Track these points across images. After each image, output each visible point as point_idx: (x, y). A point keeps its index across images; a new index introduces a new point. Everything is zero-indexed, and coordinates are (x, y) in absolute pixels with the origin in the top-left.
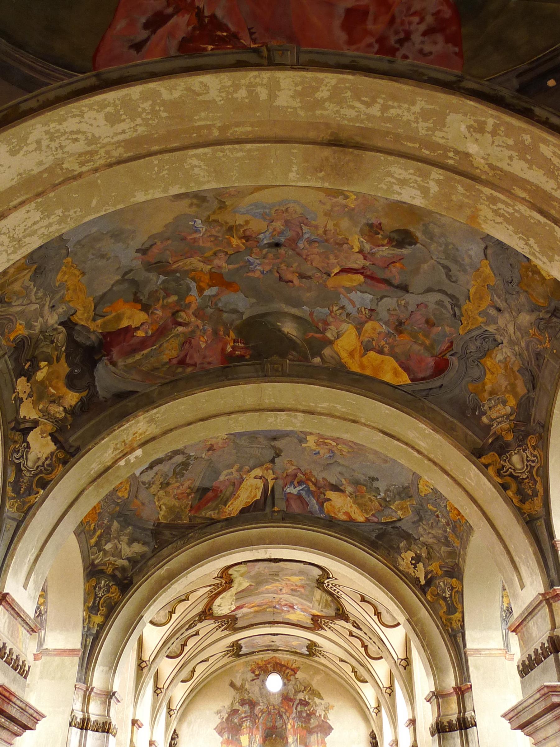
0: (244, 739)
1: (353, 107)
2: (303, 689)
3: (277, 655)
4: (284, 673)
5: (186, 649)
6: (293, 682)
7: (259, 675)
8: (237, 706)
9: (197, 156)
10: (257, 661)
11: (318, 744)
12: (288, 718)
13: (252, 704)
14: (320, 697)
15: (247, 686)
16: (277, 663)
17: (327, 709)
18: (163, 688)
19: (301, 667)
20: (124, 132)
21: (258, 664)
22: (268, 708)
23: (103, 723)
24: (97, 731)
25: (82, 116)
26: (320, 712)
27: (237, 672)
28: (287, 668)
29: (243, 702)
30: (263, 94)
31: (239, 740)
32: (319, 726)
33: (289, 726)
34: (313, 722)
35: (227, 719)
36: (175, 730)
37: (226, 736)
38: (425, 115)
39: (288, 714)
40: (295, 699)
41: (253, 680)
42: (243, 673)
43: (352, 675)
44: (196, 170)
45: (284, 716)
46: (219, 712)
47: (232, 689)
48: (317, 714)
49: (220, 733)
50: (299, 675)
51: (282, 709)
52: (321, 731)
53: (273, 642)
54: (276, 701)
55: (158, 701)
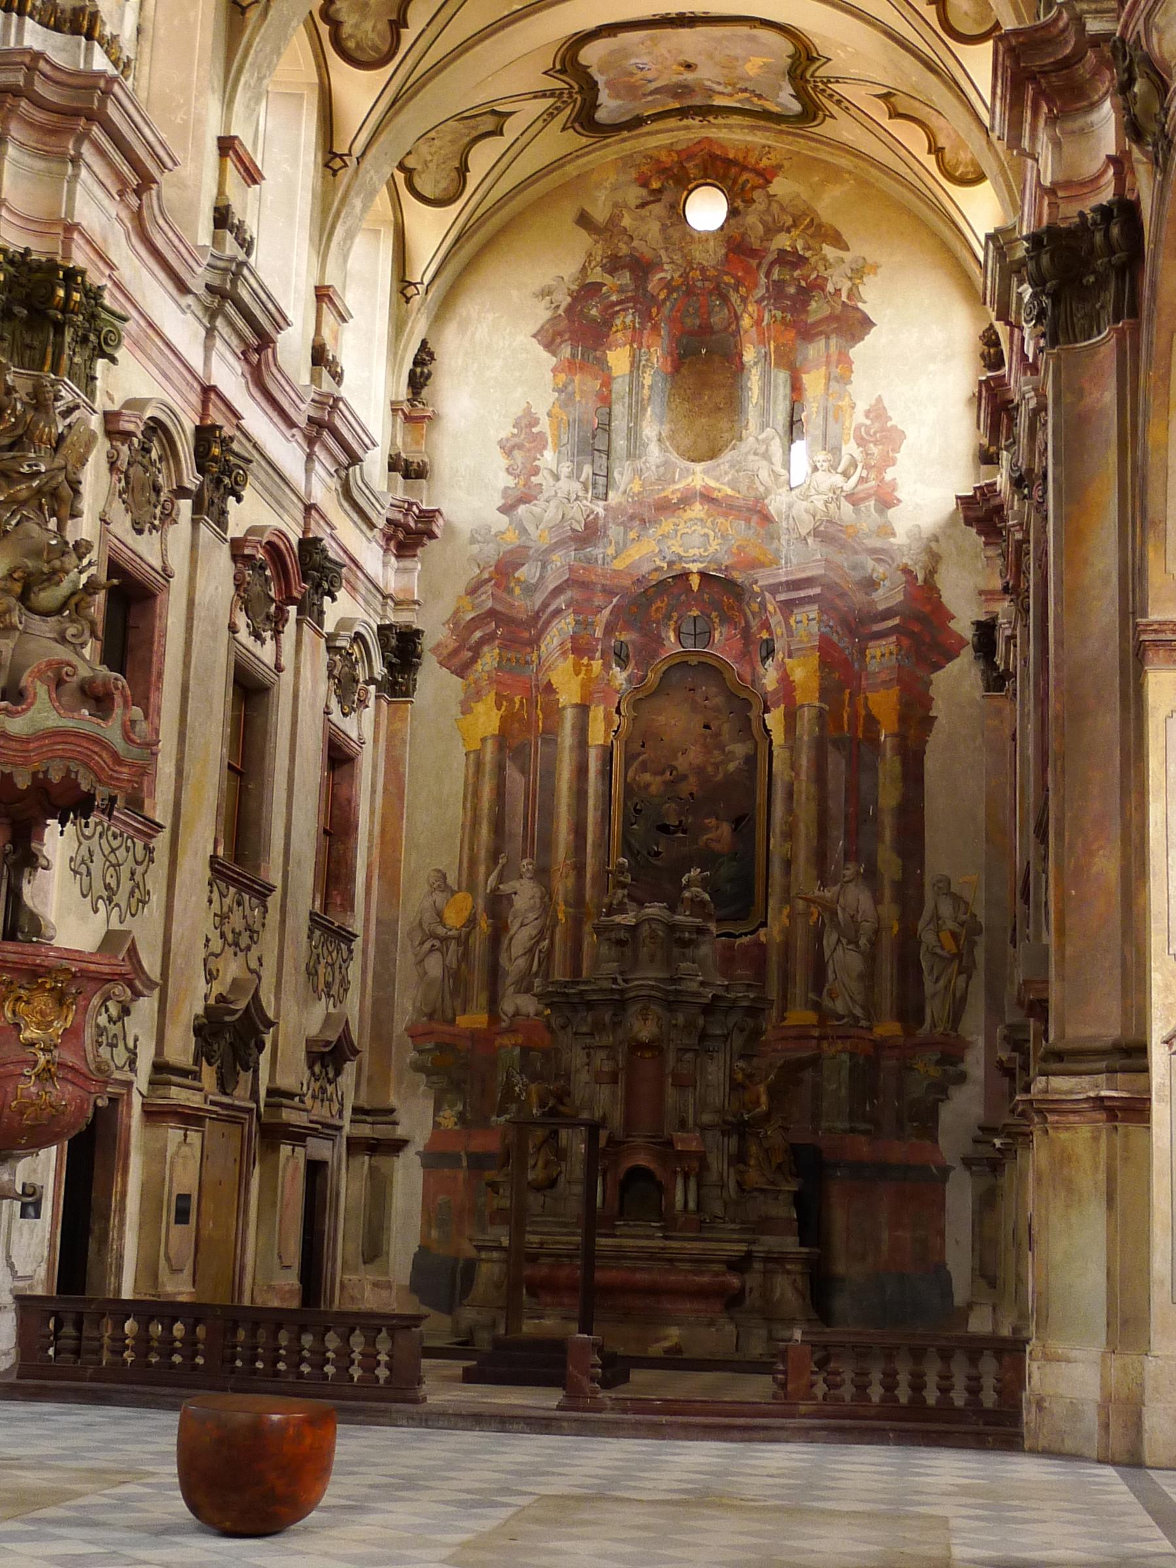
0: (618, 359)
2: (790, 222)
3: (713, 133)
4: (735, 182)
5: (408, 36)
6: (760, 205)
7: (660, 191)
8: (597, 275)
10: (655, 153)
11: (828, 363)
12: (744, 300)
13: (641, 267)
14: (838, 241)
15: (626, 222)
16: (713, 157)
17: (859, 272)
18: (350, 154)
19: (786, 164)
21: (658, 161)
22: (684, 276)
23: (74, 9)
24: (57, 28)
26: (837, 281)
27: (598, 186)
28: (744, 168)
29: (613, 265)
31: (602, 363)
32: (831, 318)
33: (746, 322)
34: (817, 309)
35: (570, 309)
36: (424, 343)
37: (566, 351)
39: (743, 290)
40: (766, 250)
41: (643, 205)
42: (615, 188)
43: (930, 161)
45: (734, 298)
46: (546, 292)
47: (583, 233)
48: (830, 288)
49: (550, 346)
50: (780, 186)
51: (726, 279)
52: (838, 331)
53: (689, 66)
54: (710, 256)
55: (335, 189)
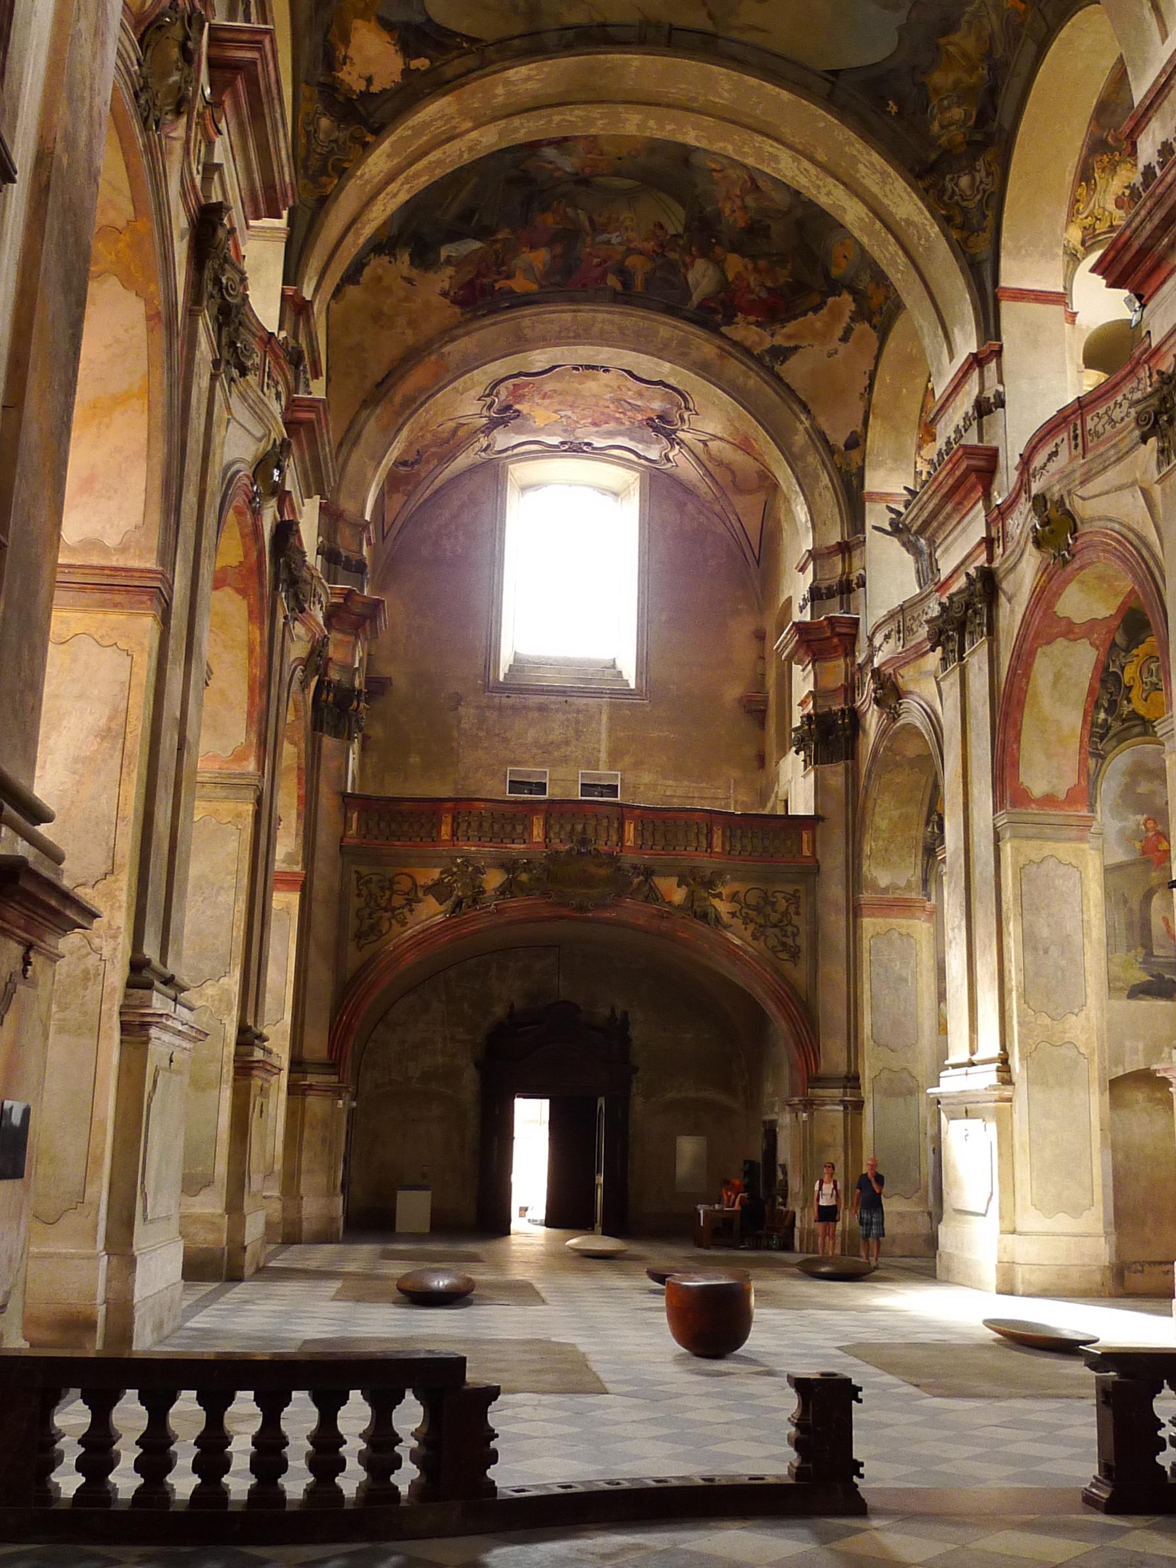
1: (577, 117)
9: (721, 97)
20: (772, 146)
25: (793, 178)
30: (652, 123)
38: (516, 130)
44: (727, 87)
